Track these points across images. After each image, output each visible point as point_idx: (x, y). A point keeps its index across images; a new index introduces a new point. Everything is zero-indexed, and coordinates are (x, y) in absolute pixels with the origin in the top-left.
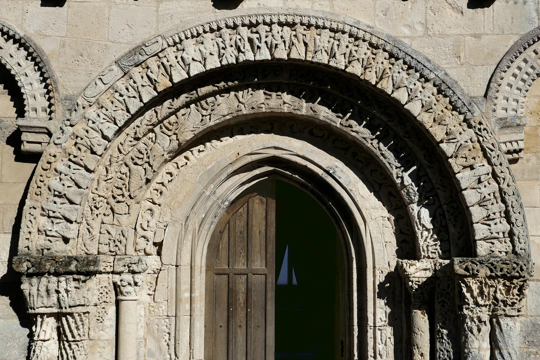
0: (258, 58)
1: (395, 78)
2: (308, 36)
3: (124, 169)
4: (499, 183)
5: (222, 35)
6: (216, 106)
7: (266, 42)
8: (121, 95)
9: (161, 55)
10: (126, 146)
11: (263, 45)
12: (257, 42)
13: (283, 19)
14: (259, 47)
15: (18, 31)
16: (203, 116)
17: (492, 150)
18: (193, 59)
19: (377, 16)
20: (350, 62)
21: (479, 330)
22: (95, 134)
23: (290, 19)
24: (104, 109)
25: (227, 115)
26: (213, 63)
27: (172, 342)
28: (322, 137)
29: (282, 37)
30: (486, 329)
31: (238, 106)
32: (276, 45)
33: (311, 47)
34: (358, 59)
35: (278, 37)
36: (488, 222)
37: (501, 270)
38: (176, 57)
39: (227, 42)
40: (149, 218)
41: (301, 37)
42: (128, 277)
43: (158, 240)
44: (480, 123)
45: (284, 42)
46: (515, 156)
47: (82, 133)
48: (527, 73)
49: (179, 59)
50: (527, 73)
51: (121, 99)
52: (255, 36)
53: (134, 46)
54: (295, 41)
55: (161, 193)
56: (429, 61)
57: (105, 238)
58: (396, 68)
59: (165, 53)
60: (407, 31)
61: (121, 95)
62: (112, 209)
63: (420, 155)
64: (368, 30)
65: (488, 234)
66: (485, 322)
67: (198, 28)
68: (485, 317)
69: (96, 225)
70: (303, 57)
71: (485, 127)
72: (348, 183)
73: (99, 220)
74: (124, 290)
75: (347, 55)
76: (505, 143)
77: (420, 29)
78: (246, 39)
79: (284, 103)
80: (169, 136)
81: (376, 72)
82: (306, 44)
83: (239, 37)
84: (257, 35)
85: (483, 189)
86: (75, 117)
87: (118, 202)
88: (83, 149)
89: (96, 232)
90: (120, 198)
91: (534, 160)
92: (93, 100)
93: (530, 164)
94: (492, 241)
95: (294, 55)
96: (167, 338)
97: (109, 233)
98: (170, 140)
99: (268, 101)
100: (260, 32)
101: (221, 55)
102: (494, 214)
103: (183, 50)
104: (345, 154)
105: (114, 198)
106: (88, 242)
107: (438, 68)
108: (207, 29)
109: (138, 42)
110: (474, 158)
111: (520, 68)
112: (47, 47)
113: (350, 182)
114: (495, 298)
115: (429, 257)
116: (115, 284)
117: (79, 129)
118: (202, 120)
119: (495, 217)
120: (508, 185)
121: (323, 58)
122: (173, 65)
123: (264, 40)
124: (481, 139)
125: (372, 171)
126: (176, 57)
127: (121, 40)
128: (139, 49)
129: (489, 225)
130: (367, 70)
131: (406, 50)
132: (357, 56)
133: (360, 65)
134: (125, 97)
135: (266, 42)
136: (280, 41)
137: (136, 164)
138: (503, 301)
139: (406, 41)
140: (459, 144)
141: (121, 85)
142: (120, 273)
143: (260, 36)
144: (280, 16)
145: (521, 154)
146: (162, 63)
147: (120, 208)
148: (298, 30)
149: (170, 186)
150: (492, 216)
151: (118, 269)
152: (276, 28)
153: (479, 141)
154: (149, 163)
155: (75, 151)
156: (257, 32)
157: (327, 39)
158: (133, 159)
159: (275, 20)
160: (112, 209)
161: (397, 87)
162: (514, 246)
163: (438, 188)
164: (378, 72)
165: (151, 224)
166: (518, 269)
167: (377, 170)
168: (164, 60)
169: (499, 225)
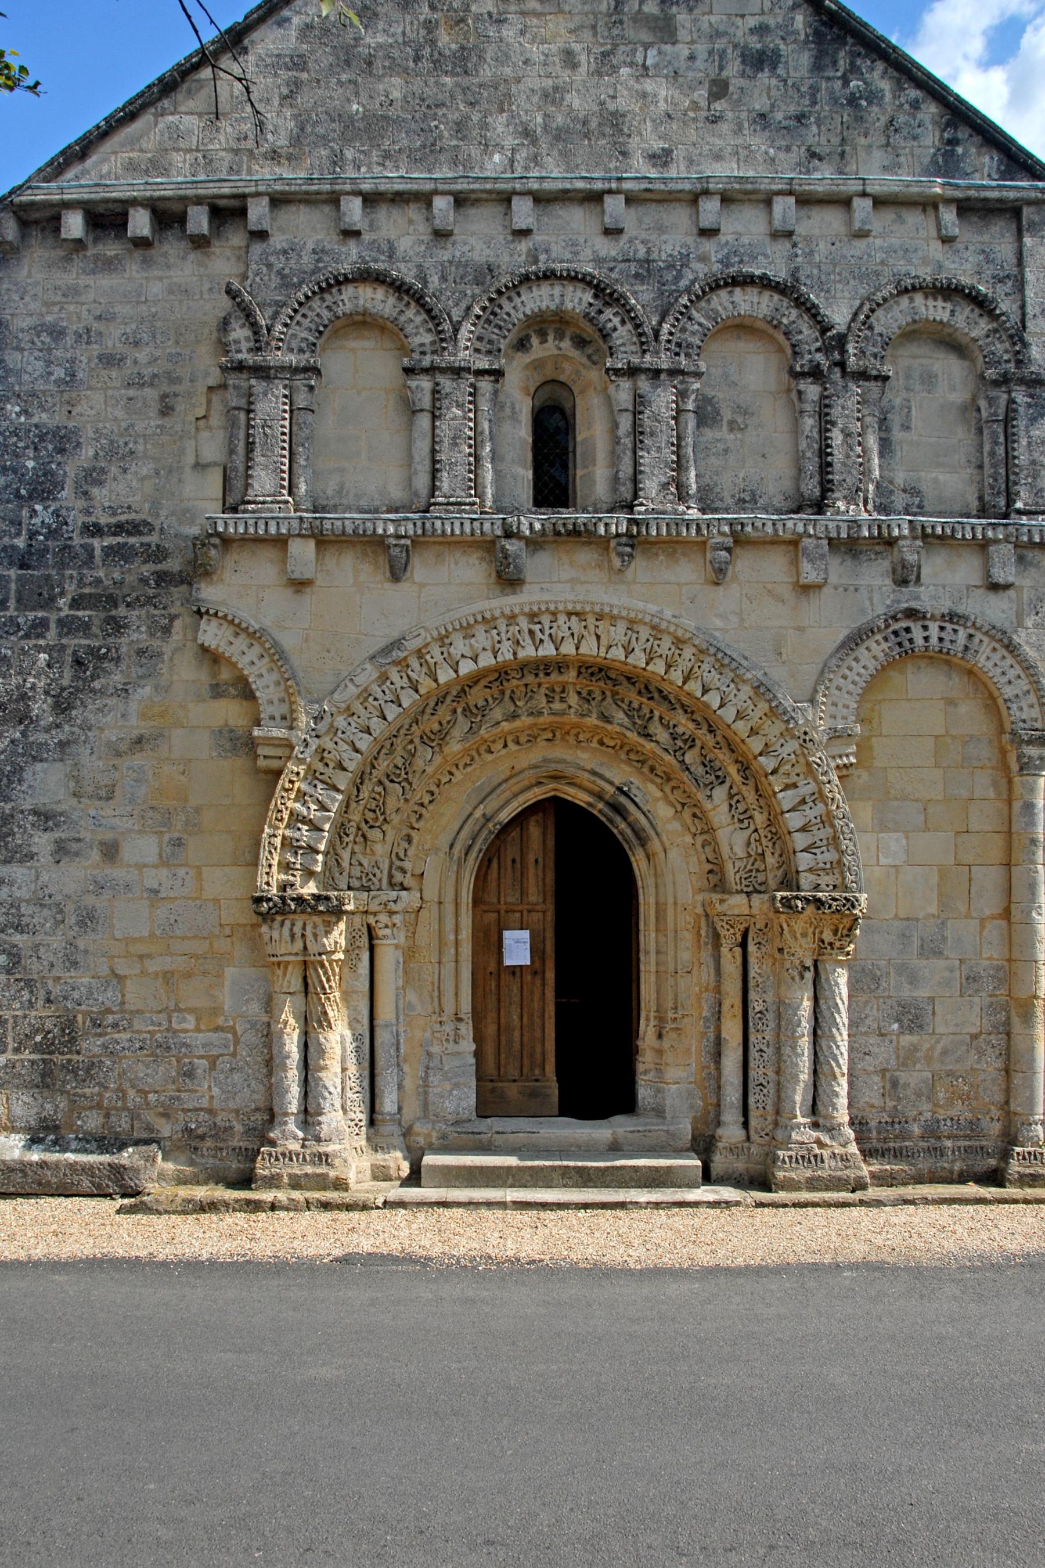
0: (541, 653)
3: (379, 789)
4: (827, 805)
8: (376, 699)
9: (424, 651)
10: (380, 760)
11: (546, 638)
12: (539, 635)
13: (570, 607)
14: (541, 641)
15: (253, 622)
18: (463, 656)
21: (802, 977)
22: (346, 747)
23: (578, 607)
24: (355, 717)
26: (486, 660)
27: (436, 993)
28: (613, 747)
30: (809, 975)
33: (604, 642)
35: (565, 627)
37: (830, 907)
40: (407, 846)
41: (592, 628)
42: (383, 918)
43: (418, 872)
44: (806, 733)
46: (844, 772)
47: (329, 745)
48: (858, 674)
49: (446, 655)
50: (858, 674)
51: (375, 703)
52: (537, 627)
53: (391, 640)
54: (585, 633)
55: (421, 816)
56: (746, 659)
57: (356, 871)
58: (706, 667)
60: (719, 623)
61: (376, 699)
62: (364, 836)
63: (733, 770)
64: (673, 620)
65: (812, 864)
66: (808, 968)
68: (809, 963)
69: (346, 855)
70: (595, 652)
73: (349, 849)
74: (381, 933)
76: (834, 758)
77: (734, 619)
79: (570, 707)
82: (598, 637)
84: (539, 626)
85: (808, 811)
86: (323, 727)
87: (371, 827)
88: (332, 765)
89: (345, 864)
90: (371, 823)
91: (865, 775)
92: (344, 706)
93: (861, 781)
96: (430, 988)
97: (361, 864)
105: (367, 822)
106: (337, 875)
107: (755, 667)
108: (480, 619)
109: (396, 635)
111: (850, 669)
112: (288, 641)
114: (823, 942)
115: (742, 891)
116: (369, 926)
117: (327, 743)
121: (618, 653)
123: (547, 632)
125: (673, 788)
127: (376, 633)
128: (397, 644)
132: (660, 651)
134: (382, 702)
136: (568, 633)
137: (392, 781)
138: (831, 944)
139: (717, 634)
141: (376, 690)
142: (375, 914)
145: (851, 771)
147: (375, 834)
149: (431, 807)
150: (819, 843)
151: (374, 907)
152: (562, 618)
154: (407, 780)
155: (320, 767)
158: (388, 776)
159: (561, 607)
160: (364, 836)
161: (705, 691)
162: (844, 879)
165: (409, 853)
166: (848, 905)
168: (428, 657)
169: (826, 854)
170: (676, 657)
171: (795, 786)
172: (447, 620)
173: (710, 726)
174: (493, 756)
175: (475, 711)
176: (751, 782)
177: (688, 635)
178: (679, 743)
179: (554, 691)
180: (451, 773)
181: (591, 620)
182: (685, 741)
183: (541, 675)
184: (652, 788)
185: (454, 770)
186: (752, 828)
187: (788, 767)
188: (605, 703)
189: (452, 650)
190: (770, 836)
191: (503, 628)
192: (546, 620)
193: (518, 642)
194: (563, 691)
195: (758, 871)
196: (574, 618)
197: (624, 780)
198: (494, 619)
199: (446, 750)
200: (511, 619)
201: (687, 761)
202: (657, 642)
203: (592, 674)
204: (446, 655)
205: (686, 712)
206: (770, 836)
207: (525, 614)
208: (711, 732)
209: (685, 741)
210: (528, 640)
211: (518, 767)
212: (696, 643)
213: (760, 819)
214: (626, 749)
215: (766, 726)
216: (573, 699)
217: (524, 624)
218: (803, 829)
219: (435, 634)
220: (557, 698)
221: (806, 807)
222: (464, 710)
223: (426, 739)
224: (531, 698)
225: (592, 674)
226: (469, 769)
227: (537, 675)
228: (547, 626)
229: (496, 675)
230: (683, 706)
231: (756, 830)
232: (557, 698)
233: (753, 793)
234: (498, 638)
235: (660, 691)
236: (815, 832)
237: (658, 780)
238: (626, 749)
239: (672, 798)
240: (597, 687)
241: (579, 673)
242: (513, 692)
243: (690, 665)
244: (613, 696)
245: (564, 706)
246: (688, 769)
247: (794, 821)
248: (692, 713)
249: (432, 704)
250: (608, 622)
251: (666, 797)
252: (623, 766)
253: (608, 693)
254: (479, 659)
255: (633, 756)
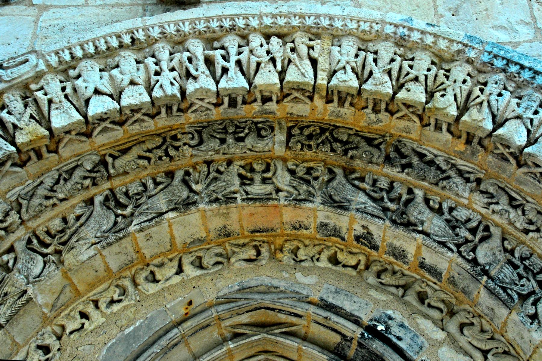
1: (494, 103)
2: (317, 48)
5: (157, 53)
6: (143, 199)
7: (239, 63)
9: (33, 87)
11: (231, 65)
12: (220, 62)
16: (117, 216)
18: (97, 92)
19: (442, 16)
20: (403, 85)
25: (167, 212)
28: (355, 267)
29: (268, 52)
31: (188, 197)
32: (258, 64)
33: (323, 64)
34: (416, 79)
35: (262, 52)
38: (63, 89)
39: (164, 65)
41: (303, 50)
45: (273, 61)
49: (69, 91)
52: (218, 53)
54: (294, 56)
59: (42, 82)
64: (430, 29)
67: (109, 39)
72: (417, 349)
75: (395, 74)
78: (202, 58)
79: (278, 190)
80: (44, 255)
81: (455, 95)
82: (314, 62)
83: (186, 54)
84: (222, 52)
95: (292, 76)
98: (45, 263)
99: (248, 188)
100: (226, 45)
101: (153, 83)
103: (79, 76)
104: (403, 296)
113: (421, 348)
118: (116, 223)
122: (56, 100)
123: (234, 58)
125: (462, 327)
126: (63, 89)
130: (438, 95)
131: (508, 56)
132: (414, 73)
133: (422, 89)
135: (239, 63)
136: (266, 58)
143: (228, 53)
144: (264, 18)
146: (35, 100)
148: (298, 41)
152: (256, 40)
156: (223, 48)
157: (354, 51)
164: (459, 95)
167: (472, 324)
170: (441, 78)
172: (74, 41)
173: (512, 199)
174: (160, 286)
175: (123, 200)
177: (456, 47)
178: (464, 233)
179: (252, 170)
180: (84, 315)
181: (301, 41)
182: (473, 231)
183: (230, 140)
184: (426, 325)
185: (90, 309)
188: (334, 183)
189: (79, 82)
191: (164, 55)
192: (232, 43)
193: (188, 75)
194: (267, 170)
196: (274, 40)
197: (376, 314)
198: (151, 42)
199: (68, 258)
200: (178, 43)
201: (481, 260)
202: (406, 64)
203: (310, 137)
204: (69, 91)
205: (468, 180)
207: (199, 35)
208: (515, 207)
209: (473, 231)
210: (203, 67)
211: (198, 301)
212: (472, 54)
214: (375, 268)
216: (283, 179)
217: (197, 48)
219: (54, 60)
220: (257, 178)
222: (107, 199)
223: (36, 244)
224: (215, 179)
225: (310, 137)
226: (116, 308)
227: (223, 141)
228: (233, 51)
229: (159, 141)
230: (460, 173)
232: (257, 178)
234: (153, 68)
235: (421, 156)
237: (436, 314)
238: (375, 268)
239: (463, 341)
240: (320, 156)
241: (290, 136)
242: (187, 173)
243: (466, 88)
244: (346, 176)
245: (269, 188)
246: (485, 272)
248: (479, 181)
249: (49, 182)
250: (327, 42)
251: (453, 341)
252: (373, 293)
253: (338, 171)
254: (124, 96)
255: (386, 279)
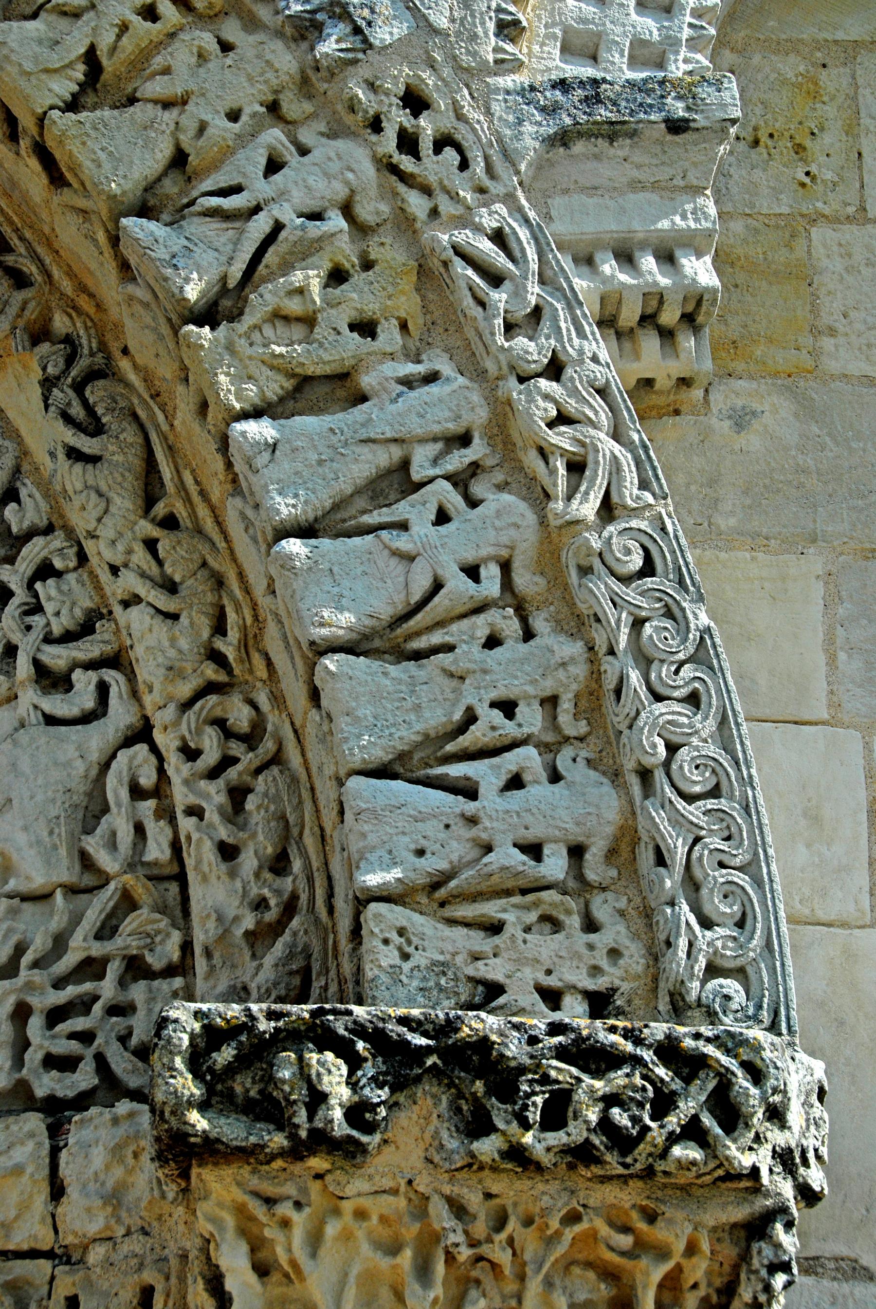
17: (496, 279)
36: (456, 770)
37: (558, 1111)
44: (415, 102)
65: (455, 849)
71: (447, 123)
76: (587, 261)
93: (752, 441)
94: (491, 909)
102: (508, 708)
110: (365, 328)
119: (510, 729)
120: (608, 509)
124: (417, 203)
129: (468, 791)
140: (261, 225)
150: (490, 725)
153: (404, 222)
162: (658, 950)
163: (131, 601)
169: (539, 791)
171: (341, 388)
176: (119, 449)
186: (121, 715)
187: (311, 278)
190: (211, 747)
195: (136, 968)
206: (211, 747)
213: (162, 649)
215: (180, 56)
218: (390, 641)
221: (416, 510)
231: (142, 734)
233: (124, 503)
236: (469, 654)
247: (336, 592)
